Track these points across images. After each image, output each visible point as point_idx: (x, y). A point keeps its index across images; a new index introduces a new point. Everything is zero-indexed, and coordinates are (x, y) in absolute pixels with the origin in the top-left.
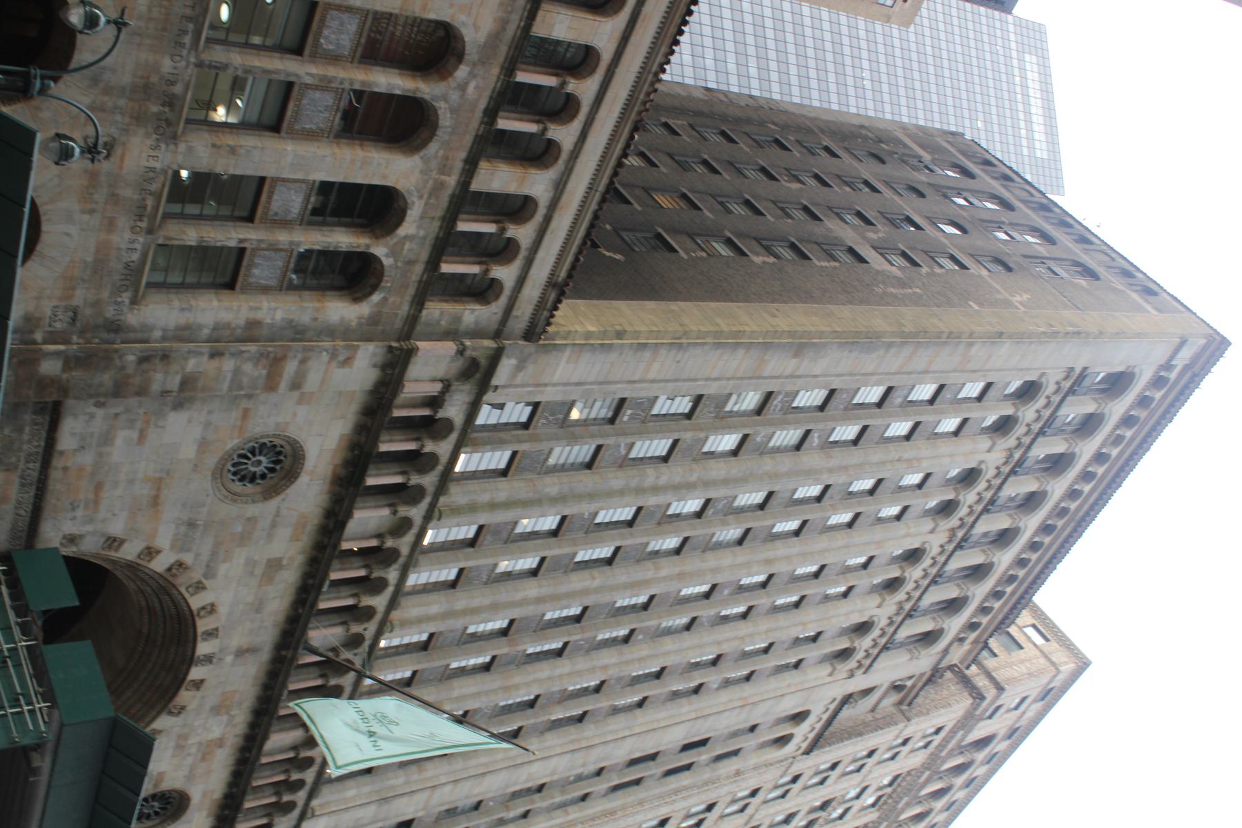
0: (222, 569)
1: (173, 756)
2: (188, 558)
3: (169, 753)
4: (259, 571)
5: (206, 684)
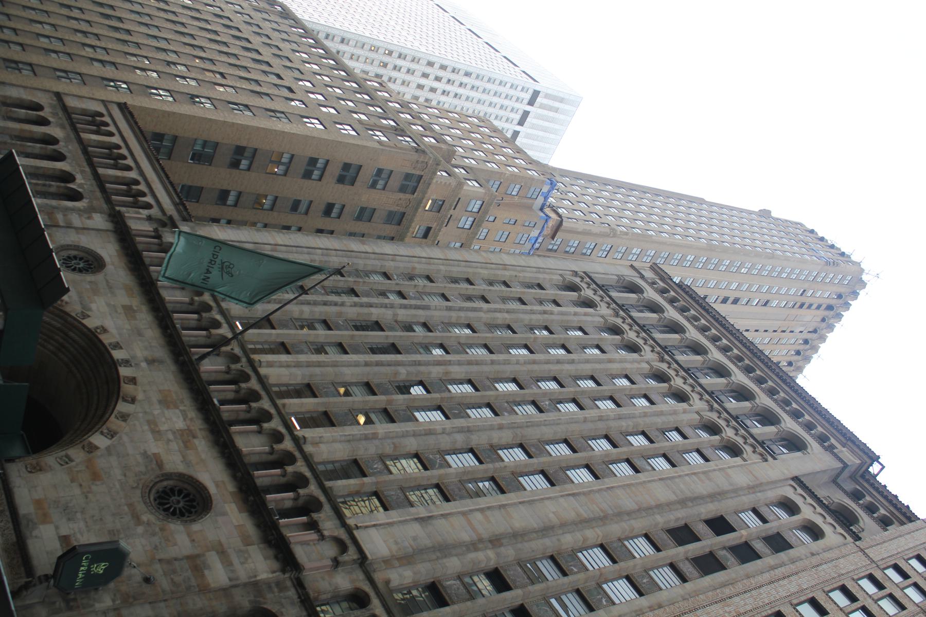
0: (94, 306)
1: (156, 440)
3: (150, 436)
4: (120, 310)
5: (139, 380)
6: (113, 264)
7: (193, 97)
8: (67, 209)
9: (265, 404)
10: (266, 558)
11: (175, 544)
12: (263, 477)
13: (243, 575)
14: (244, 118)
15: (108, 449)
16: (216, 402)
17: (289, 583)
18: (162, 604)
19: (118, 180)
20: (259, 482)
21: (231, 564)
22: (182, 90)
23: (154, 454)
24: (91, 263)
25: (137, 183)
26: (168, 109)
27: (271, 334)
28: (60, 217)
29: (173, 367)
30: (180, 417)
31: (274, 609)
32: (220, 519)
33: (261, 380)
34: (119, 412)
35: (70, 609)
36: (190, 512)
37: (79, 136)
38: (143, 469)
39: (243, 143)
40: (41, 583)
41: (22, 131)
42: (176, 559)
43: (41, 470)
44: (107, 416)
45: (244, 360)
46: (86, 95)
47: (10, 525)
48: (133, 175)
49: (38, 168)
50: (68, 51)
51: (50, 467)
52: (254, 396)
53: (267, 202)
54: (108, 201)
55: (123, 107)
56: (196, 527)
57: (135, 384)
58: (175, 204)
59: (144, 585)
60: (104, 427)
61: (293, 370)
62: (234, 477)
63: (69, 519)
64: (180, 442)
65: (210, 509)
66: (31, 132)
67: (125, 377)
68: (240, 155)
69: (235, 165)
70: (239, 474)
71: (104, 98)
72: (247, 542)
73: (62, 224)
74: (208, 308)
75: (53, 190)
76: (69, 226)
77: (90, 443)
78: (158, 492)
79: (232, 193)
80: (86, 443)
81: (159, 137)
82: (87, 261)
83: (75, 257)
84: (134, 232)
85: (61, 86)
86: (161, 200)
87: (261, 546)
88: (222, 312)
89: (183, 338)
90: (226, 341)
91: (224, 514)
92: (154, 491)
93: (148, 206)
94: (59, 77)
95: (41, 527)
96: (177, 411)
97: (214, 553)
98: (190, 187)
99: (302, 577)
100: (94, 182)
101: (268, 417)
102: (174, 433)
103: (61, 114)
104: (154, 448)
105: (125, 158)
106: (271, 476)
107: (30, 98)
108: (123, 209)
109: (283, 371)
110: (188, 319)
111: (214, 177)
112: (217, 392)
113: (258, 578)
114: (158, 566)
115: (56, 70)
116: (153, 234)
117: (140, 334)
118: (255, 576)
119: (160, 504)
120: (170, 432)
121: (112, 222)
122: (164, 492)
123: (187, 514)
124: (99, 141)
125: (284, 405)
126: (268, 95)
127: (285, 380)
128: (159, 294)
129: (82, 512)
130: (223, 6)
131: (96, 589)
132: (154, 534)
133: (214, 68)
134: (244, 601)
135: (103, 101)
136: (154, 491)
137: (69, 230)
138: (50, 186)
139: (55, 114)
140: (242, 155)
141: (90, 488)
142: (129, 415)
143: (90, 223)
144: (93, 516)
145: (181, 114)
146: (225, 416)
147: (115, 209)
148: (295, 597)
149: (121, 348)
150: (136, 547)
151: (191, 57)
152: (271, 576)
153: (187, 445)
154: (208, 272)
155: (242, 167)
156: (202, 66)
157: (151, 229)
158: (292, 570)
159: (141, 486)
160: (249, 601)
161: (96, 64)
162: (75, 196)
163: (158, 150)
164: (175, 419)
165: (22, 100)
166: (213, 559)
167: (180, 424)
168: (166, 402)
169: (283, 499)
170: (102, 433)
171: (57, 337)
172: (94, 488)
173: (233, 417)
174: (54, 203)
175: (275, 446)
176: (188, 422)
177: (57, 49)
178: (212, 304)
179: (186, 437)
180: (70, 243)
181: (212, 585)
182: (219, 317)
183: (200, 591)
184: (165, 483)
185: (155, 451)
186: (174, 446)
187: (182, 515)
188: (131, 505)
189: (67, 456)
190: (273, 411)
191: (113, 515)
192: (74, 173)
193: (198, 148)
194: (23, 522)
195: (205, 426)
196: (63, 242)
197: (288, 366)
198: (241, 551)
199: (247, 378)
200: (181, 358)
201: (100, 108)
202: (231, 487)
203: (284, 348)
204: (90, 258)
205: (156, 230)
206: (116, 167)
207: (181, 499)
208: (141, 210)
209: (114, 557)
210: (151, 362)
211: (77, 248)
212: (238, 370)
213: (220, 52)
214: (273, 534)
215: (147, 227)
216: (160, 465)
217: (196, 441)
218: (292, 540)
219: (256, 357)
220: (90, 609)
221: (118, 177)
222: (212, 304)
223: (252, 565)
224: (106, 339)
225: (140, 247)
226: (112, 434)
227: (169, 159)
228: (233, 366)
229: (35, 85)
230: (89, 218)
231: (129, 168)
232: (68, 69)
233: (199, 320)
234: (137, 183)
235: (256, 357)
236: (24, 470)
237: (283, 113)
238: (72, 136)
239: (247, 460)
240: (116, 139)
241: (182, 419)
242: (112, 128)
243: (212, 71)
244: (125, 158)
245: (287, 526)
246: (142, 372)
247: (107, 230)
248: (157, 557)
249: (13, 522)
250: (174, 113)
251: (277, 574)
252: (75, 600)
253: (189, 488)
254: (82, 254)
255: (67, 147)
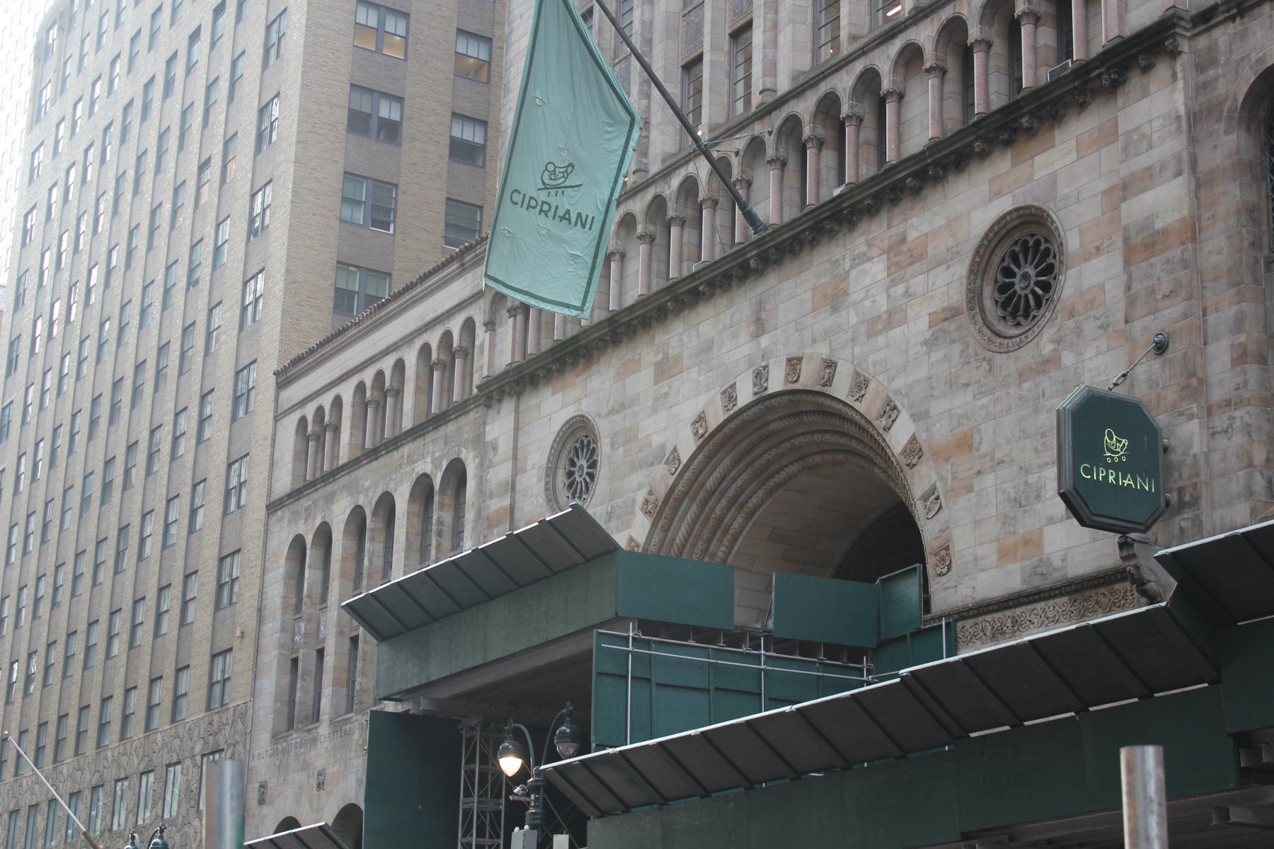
0: (657, 440)
2: (641, 496)
3: (896, 333)
5: (793, 352)
6: (578, 401)
7: (252, 232)
8: (480, 490)
9: (844, 82)
10: (1145, 94)
11: (1102, 286)
12: (990, 93)
13: (1171, 146)
14: (285, 115)
15: (916, 418)
16: (837, 192)
17: (1202, 42)
18: (1211, 318)
19: (425, 390)
20: (998, 101)
21: (1149, 169)
22: (241, 255)
23: (932, 324)
24: (578, 444)
25: (426, 349)
26: (281, 285)
27: (712, 63)
28: (498, 504)
29: (771, 280)
30: (862, 265)
31: (1249, 77)
32: (1063, 190)
33: (796, 93)
34: (851, 393)
35: (1196, 501)
36: (1047, 251)
37: (344, 465)
38: (957, 348)
39: (343, 115)
40: (1134, 556)
41: (343, 575)
42: (1129, 288)
43: (947, 548)
44: (858, 417)
45: (758, 129)
46: (268, 452)
47: (1040, 606)
48: (411, 357)
49: (409, 547)
50: (189, 489)
51: (942, 531)
52: (829, 104)
53: (475, 51)
54: (461, 409)
55: (284, 378)
56: (1072, 243)
57: (800, 359)
58: (463, 270)
59: (1169, 355)
60: (876, 423)
61: (783, 15)
62: (983, 156)
63: (1038, 497)
64: (910, 270)
65: (1042, 211)
66: (344, 559)
67: (787, 381)
68: (370, 123)
69: (391, 131)
70: (978, 146)
71: (271, 416)
72: (1108, 135)
73: (507, 502)
74: (658, 203)
75: (448, 517)
76: (512, 487)
77: (904, 451)
78: (1004, 318)
79: (457, 133)
80: (903, 461)
81: (343, 299)
82: (576, 450)
83: (570, 474)
84: (518, 358)
85: (255, 500)
86: (456, 301)
87: (1120, 101)
88: (666, 174)
89: (717, 257)
90: (720, 168)
91: (1053, 180)
92: (1001, 327)
93: (469, 326)
94: (239, 506)
95: (1047, 550)
96: (853, 274)
97: (1124, 205)
98: (448, 225)
99: (1194, 12)
100: (429, 437)
101: (869, 79)
102: (893, 283)
103: (306, 502)
104: (918, 326)
105: (380, 375)
106: (986, 74)
107: (282, 562)
108: (477, 380)
109: (785, 38)
110: (681, 245)
111: (423, 177)
112: (824, 187)
113: (1182, 111)
114: (1137, 325)
115: (226, 512)
116: (520, 318)
117: (707, 348)
118: (1178, 117)
119: (1026, 316)
120: (891, 291)
121: (500, 401)
122: (1004, 305)
123: (1050, 260)
124: (352, 427)
125: (853, 38)
126: (234, 63)
127: (805, 33)
128: (631, 309)
129: (1027, 472)
130: (65, 165)
131: (1166, 450)
132: (1079, 331)
133: (192, 184)
134: (1229, 144)
135: (276, 419)
136: (1001, 327)
137: (518, 487)
138: (440, 523)
139: (309, 515)
140: (369, 116)
141: (985, 456)
142: (857, 374)
143: (505, 446)
144: (1036, 450)
145: (289, 257)
146: (868, 171)
147: (476, 398)
148: (1231, 28)
149: (733, 386)
150: (1099, 366)
151: (174, 233)
152: (1180, 84)
153: (917, 257)
154: (566, 217)
155: (395, 116)
156: (190, 210)
157: (511, 321)
158: (1174, 36)
159: (988, 354)
160: (1226, 133)
161: (207, 434)
162: (456, 473)
163: (370, 299)
164: (868, 281)
165: (288, 576)
166: (1136, 208)
167: (877, 269)
168: (834, 299)
169: (1035, 49)
170: (887, 429)
171: (718, 511)
172: (985, 448)
173: (869, 154)
174: (470, 515)
175: (927, 65)
176: (875, 251)
177: (187, 509)
178: (649, 195)
179: (904, 258)
180: (542, 484)
181: (1185, 213)
182: (676, 181)
183: (1193, 239)
184: (988, 304)
185: (923, 324)
186: (917, 283)
187: (1049, 270)
188: (1022, 377)
189: (925, 498)
190: (858, 67)
191: (1036, 410)
192: (414, 477)
193: (359, 215)
194: (1038, 583)
195: (884, 215)
196: (542, 500)
197: (775, 27)
198: (1125, 149)
199: (793, 123)
200: (752, 263)
201: (291, 422)
202: (1001, 164)
203: (741, 33)
204: (569, 445)
205: (513, 312)
206: (398, 393)
207: (1019, 270)
208: (477, 342)
209: (1094, 418)
210: (760, 326)
211: (551, 472)
212: (778, 143)
213: (158, 169)
214: (1099, 76)
215: (507, 329)
216: (951, 313)
217: (912, 236)
218: (1114, 33)
219: (756, 100)
220: (1202, 461)
221: (418, 390)
222: (649, 195)
223: (1155, 124)
224: (716, 417)
225: (546, 345)
226: (890, 409)
227: (390, 275)
228: (770, 153)
229: (258, 552)
230: (495, 448)
231: (400, 366)
232: (222, 489)
233: (683, 223)
234: (426, 349)
235: (756, 100)
236: (944, 579)
237: (268, 28)
238: (345, 479)
239: (954, 125)
240: (347, 391)
241: (867, 265)
242: (326, 401)
243: (199, 189)
244: (380, 375)
245: (1087, 42)
246: (778, 346)
247: (517, 412)
248: (1122, 326)
249: (1035, 601)
250: (288, 271)
251: (1178, 68)
252: (1180, 491)
253: (1000, 252)
254: (564, 462)
255: (366, 490)
